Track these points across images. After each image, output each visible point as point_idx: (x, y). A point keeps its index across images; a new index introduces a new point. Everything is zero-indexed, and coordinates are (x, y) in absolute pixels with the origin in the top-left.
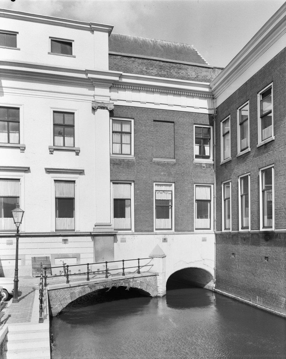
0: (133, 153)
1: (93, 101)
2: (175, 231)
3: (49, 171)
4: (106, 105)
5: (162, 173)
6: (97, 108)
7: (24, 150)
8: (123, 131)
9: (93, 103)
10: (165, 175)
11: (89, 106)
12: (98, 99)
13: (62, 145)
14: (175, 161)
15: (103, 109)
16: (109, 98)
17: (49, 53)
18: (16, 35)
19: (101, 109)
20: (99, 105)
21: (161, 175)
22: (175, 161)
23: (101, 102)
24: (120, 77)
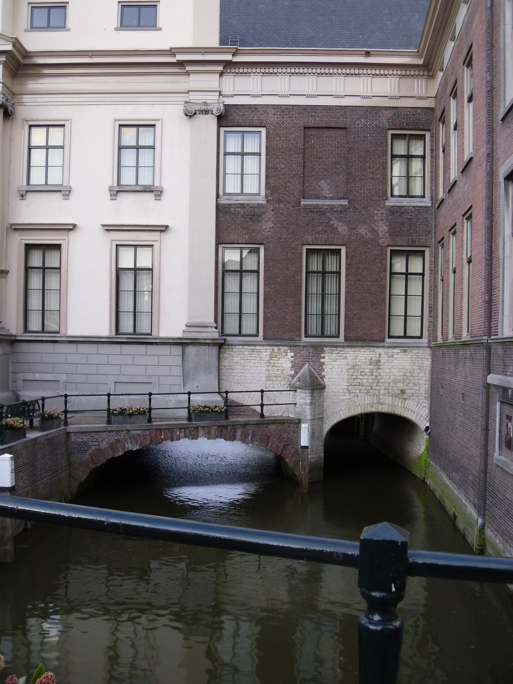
0: (263, 192)
1: (186, 102)
2: (345, 340)
3: (109, 229)
4: (209, 108)
5: (320, 228)
6: (193, 113)
7: (68, 195)
8: (245, 151)
9: (186, 105)
10: (326, 231)
11: (179, 110)
12: (194, 97)
13: (134, 183)
14: (346, 203)
15: (205, 114)
16: (218, 94)
17: (116, 29)
18: (66, 6)
19: (203, 114)
20: (197, 108)
21: (318, 233)
22: (346, 203)
23: (200, 101)
24: (234, 55)
